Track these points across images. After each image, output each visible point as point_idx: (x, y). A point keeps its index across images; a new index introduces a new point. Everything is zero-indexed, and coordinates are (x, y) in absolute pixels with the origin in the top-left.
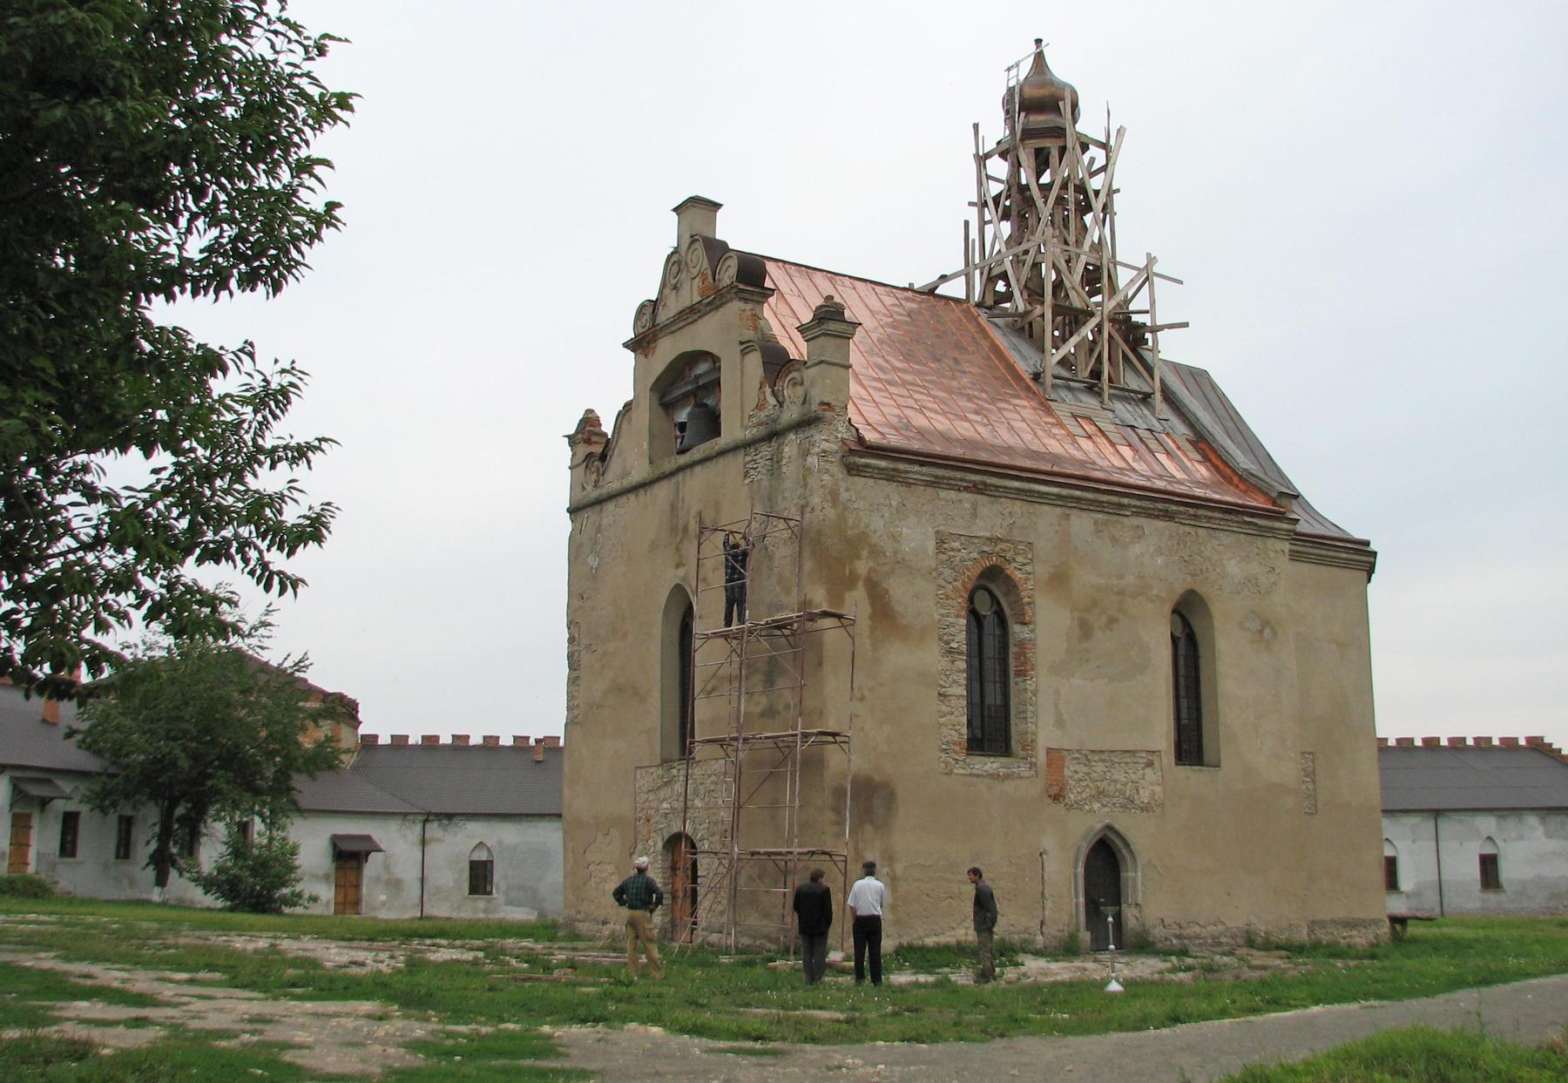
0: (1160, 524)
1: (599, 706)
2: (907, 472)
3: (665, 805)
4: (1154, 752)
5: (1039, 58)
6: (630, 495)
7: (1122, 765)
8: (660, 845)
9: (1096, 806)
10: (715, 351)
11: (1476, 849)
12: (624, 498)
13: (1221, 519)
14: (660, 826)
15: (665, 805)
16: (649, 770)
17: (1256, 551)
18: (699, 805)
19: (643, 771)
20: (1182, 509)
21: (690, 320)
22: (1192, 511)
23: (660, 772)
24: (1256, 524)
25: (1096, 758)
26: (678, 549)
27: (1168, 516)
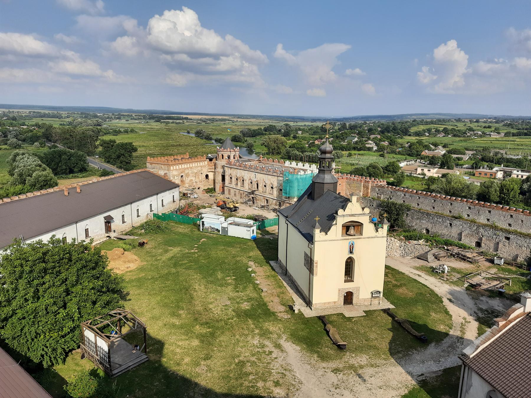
8: (343, 294)
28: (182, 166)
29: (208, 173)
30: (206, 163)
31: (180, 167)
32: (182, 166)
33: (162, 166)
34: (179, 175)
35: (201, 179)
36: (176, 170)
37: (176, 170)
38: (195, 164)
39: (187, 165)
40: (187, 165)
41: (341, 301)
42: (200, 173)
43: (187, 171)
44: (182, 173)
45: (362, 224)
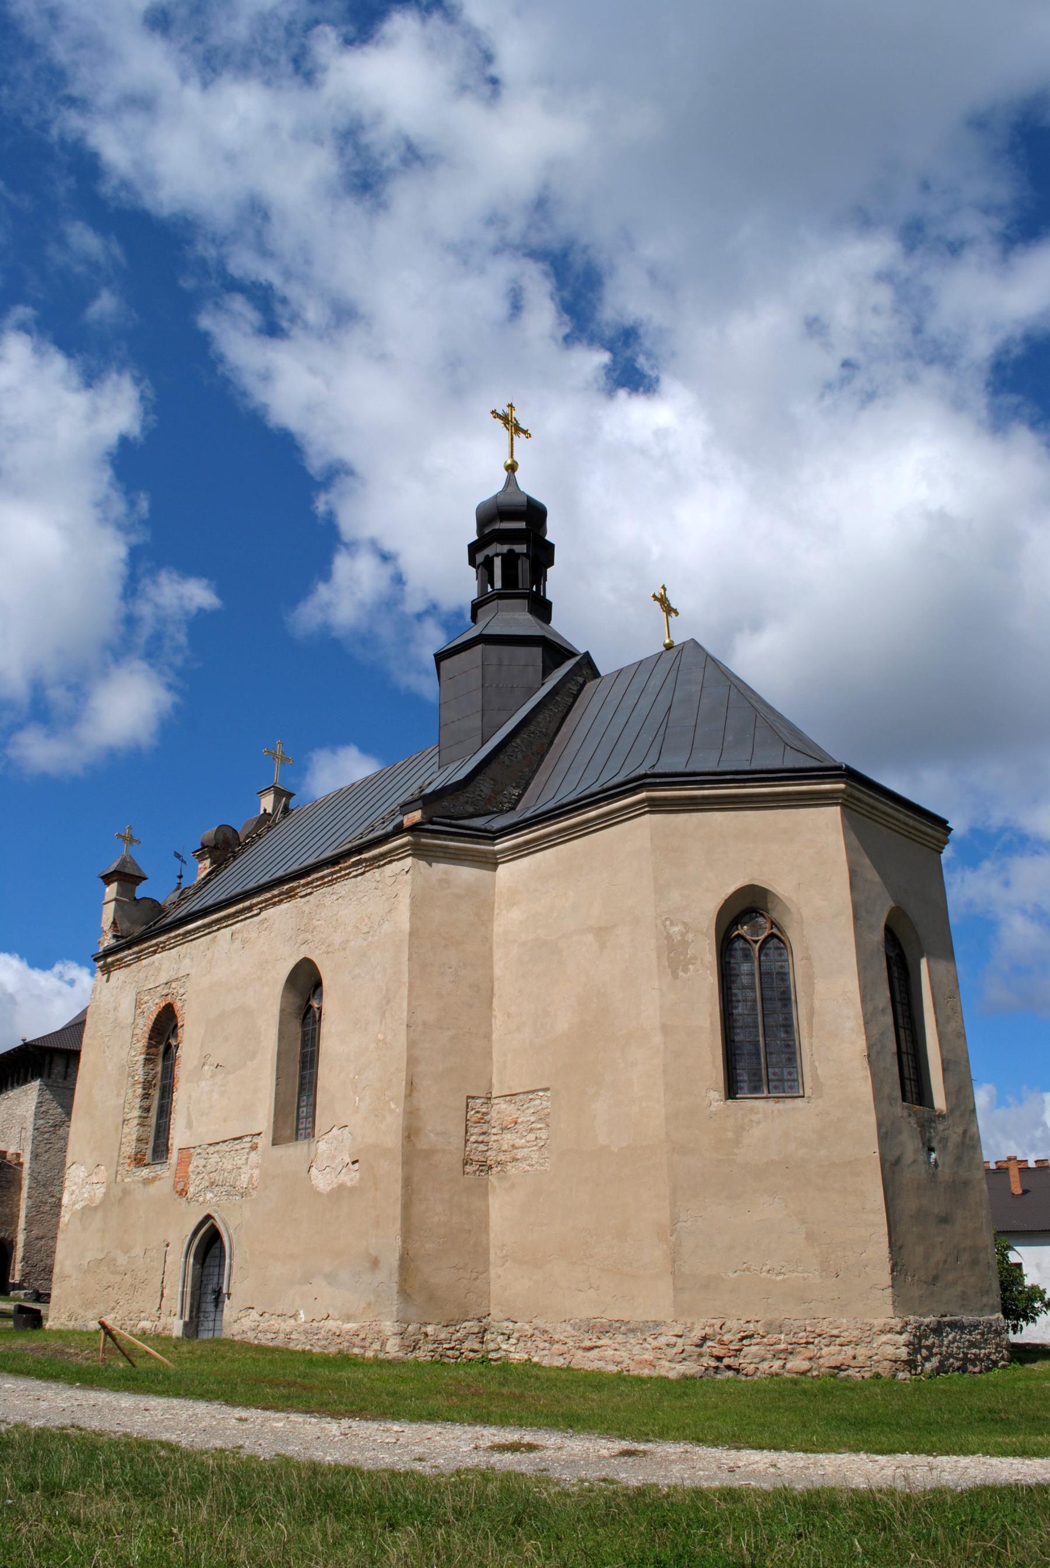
0: (283, 906)
2: (122, 959)
4: (259, 1134)
7: (232, 1153)
9: (209, 1195)
13: (332, 873)
17: (374, 885)
20: (294, 884)
22: (302, 882)
24: (366, 860)
25: (212, 1149)
27: (290, 895)
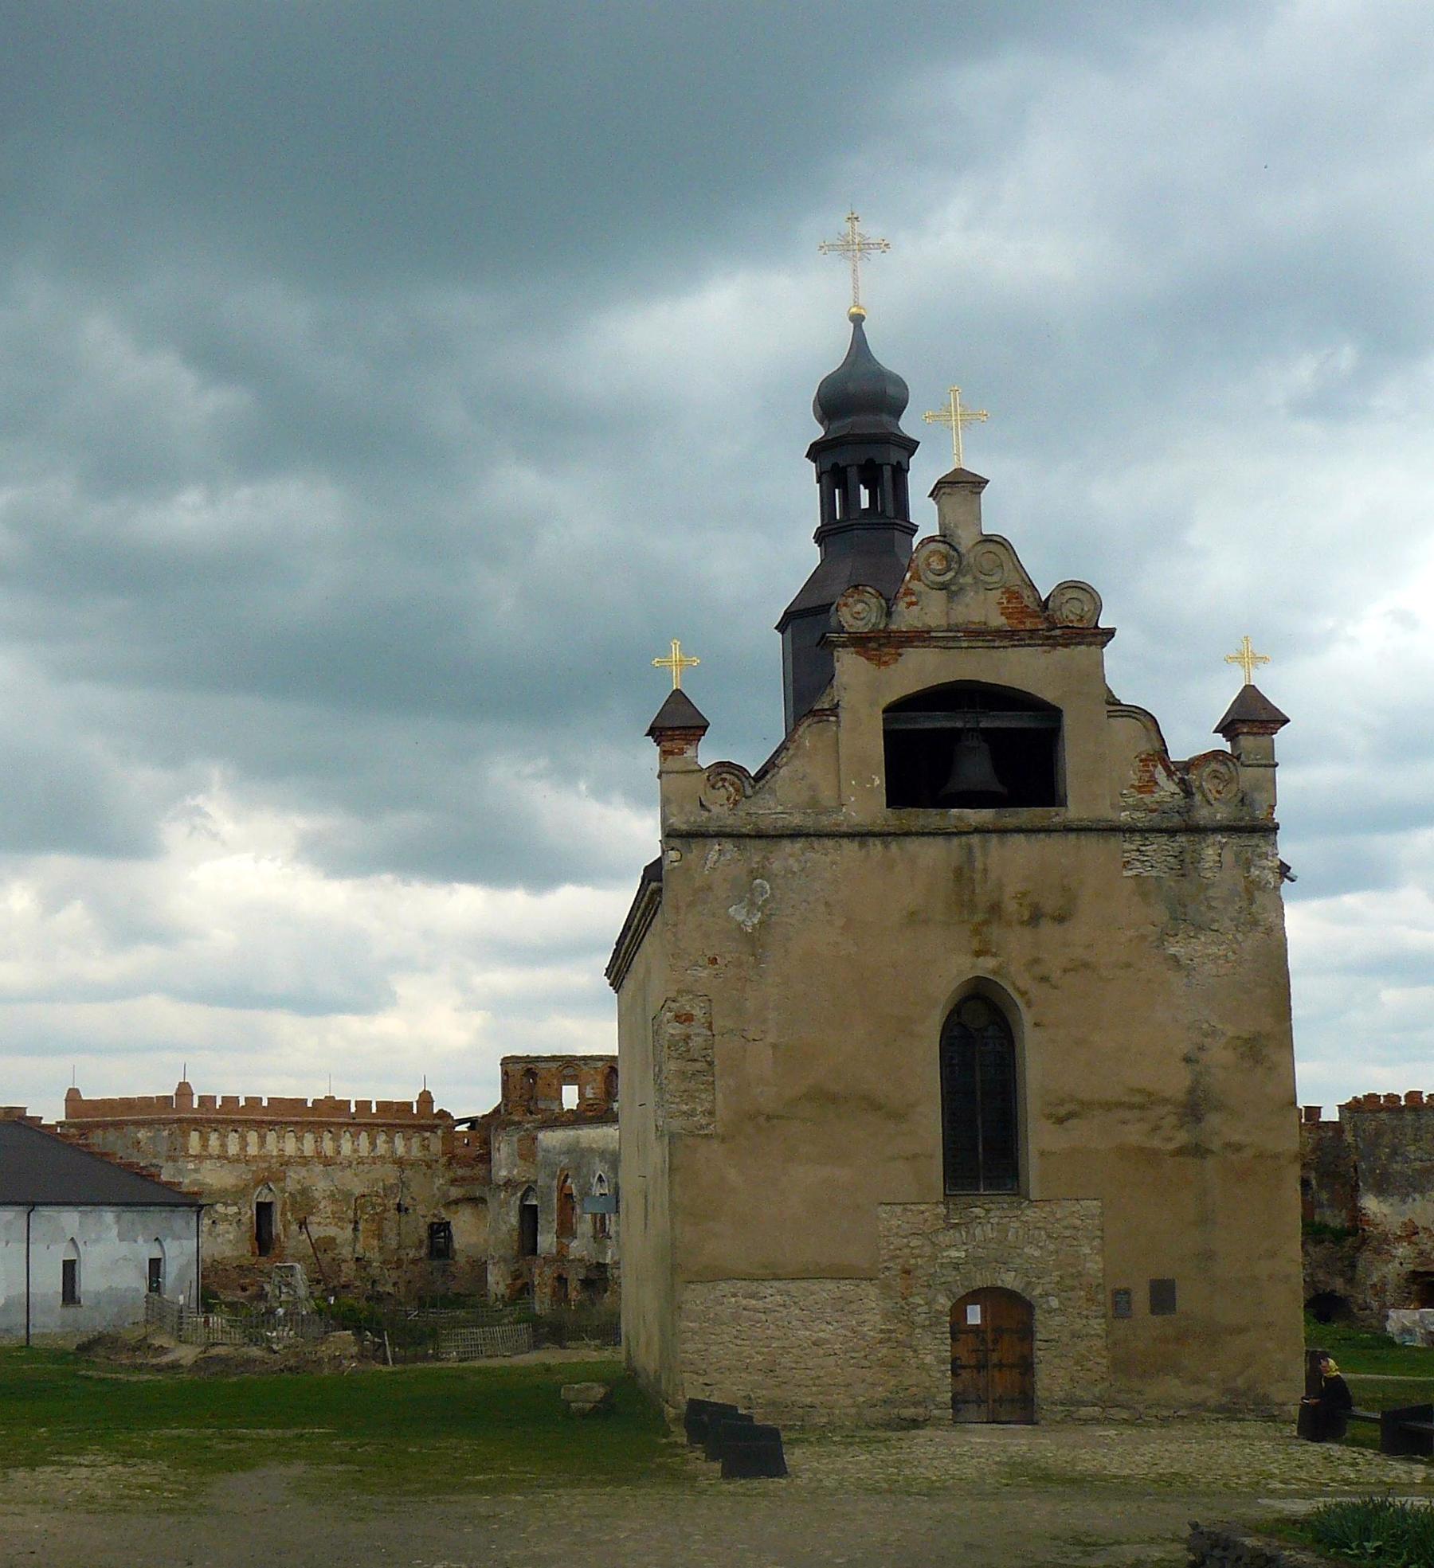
1: (769, 1118)
3: (954, 1253)
5: (859, 343)
6: (845, 842)
8: (944, 1302)
10: (1049, 695)
11: (63, 1252)
12: (829, 843)
14: (943, 1280)
15: (954, 1253)
16: (909, 1207)
18: (1037, 1254)
19: (898, 1209)
21: (996, 644)
23: (942, 1210)
26: (976, 931)
28: (262, 1139)
29: (445, 1215)
30: (436, 1145)
31: (253, 1150)
32: (262, 1139)
33: (142, 1134)
34: (237, 1195)
35: (394, 1244)
36: (219, 1157)
37: (223, 1157)
38: (355, 1137)
39: (300, 1139)
40: (300, 1139)
41: (923, 1367)
42: (392, 1203)
43: (294, 1178)
44: (264, 1182)
45: (1052, 714)
